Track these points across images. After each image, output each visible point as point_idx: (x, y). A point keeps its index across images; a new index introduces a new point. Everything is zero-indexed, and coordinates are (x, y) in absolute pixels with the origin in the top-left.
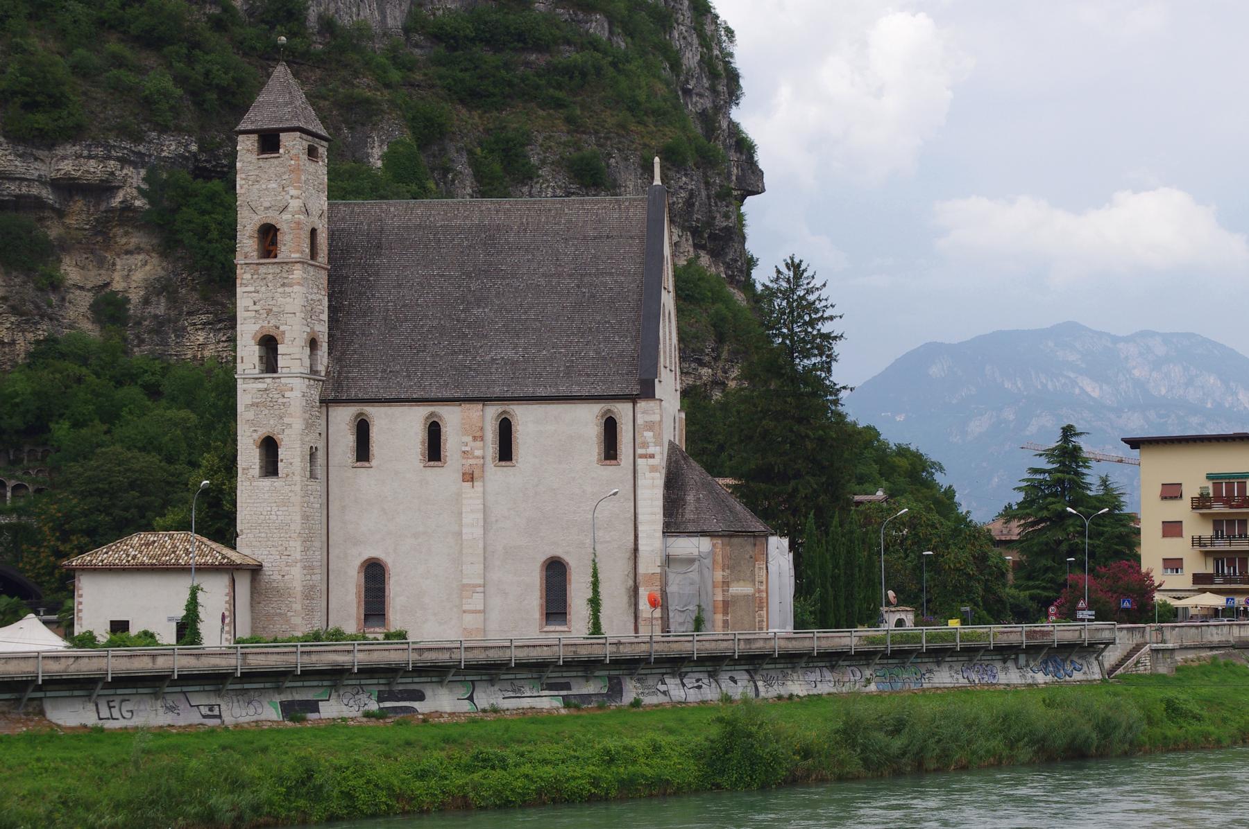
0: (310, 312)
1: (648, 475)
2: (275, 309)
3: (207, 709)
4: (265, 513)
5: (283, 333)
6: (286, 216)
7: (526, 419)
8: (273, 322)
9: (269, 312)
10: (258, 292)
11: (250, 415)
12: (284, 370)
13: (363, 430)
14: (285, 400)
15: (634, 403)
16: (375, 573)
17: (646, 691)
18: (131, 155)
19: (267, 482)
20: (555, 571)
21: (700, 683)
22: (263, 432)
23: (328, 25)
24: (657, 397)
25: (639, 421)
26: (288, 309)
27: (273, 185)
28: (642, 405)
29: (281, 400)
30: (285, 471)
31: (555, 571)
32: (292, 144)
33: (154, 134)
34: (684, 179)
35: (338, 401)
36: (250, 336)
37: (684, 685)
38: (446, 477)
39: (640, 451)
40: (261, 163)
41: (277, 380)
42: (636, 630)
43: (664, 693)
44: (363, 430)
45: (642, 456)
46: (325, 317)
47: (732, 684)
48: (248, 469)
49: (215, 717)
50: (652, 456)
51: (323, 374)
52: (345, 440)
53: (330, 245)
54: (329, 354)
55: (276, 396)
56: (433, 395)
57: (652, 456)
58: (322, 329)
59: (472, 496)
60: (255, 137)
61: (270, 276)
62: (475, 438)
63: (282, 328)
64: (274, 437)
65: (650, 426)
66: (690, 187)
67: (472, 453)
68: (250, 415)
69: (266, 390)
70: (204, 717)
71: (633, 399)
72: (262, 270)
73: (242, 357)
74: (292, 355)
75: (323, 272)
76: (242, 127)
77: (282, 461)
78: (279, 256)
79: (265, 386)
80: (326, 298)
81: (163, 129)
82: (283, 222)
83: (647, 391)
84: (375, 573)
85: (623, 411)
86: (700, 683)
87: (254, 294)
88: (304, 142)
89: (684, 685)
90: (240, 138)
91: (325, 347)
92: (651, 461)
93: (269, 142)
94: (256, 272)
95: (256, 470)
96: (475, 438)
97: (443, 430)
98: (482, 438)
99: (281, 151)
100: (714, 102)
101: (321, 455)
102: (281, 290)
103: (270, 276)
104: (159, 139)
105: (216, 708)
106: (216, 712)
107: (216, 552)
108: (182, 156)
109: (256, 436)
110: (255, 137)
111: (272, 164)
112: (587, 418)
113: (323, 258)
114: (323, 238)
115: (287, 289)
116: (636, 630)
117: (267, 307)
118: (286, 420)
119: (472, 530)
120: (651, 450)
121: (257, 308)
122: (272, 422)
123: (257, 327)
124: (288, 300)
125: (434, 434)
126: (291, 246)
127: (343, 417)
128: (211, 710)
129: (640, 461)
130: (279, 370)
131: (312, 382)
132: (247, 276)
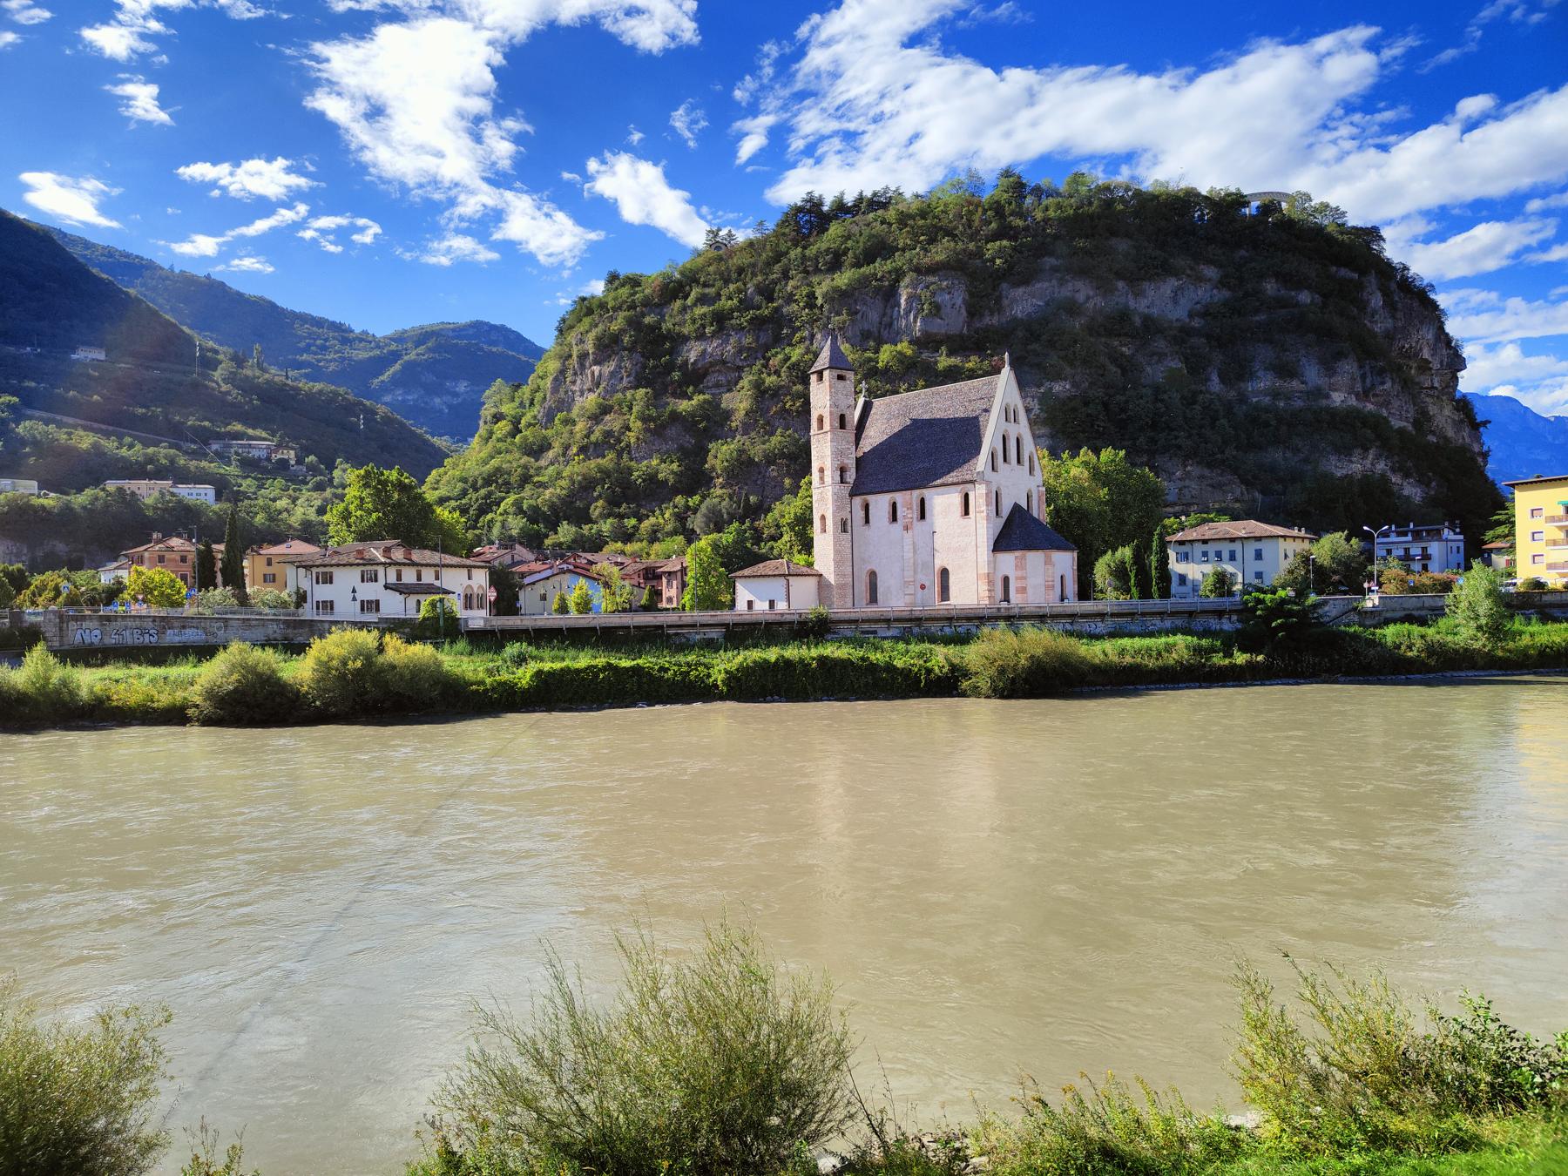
13: (867, 508)
38: (898, 526)
52: (859, 514)
59: (908, 537)
119: (909, 555)
125: (894, 506)
127: (858, 501)
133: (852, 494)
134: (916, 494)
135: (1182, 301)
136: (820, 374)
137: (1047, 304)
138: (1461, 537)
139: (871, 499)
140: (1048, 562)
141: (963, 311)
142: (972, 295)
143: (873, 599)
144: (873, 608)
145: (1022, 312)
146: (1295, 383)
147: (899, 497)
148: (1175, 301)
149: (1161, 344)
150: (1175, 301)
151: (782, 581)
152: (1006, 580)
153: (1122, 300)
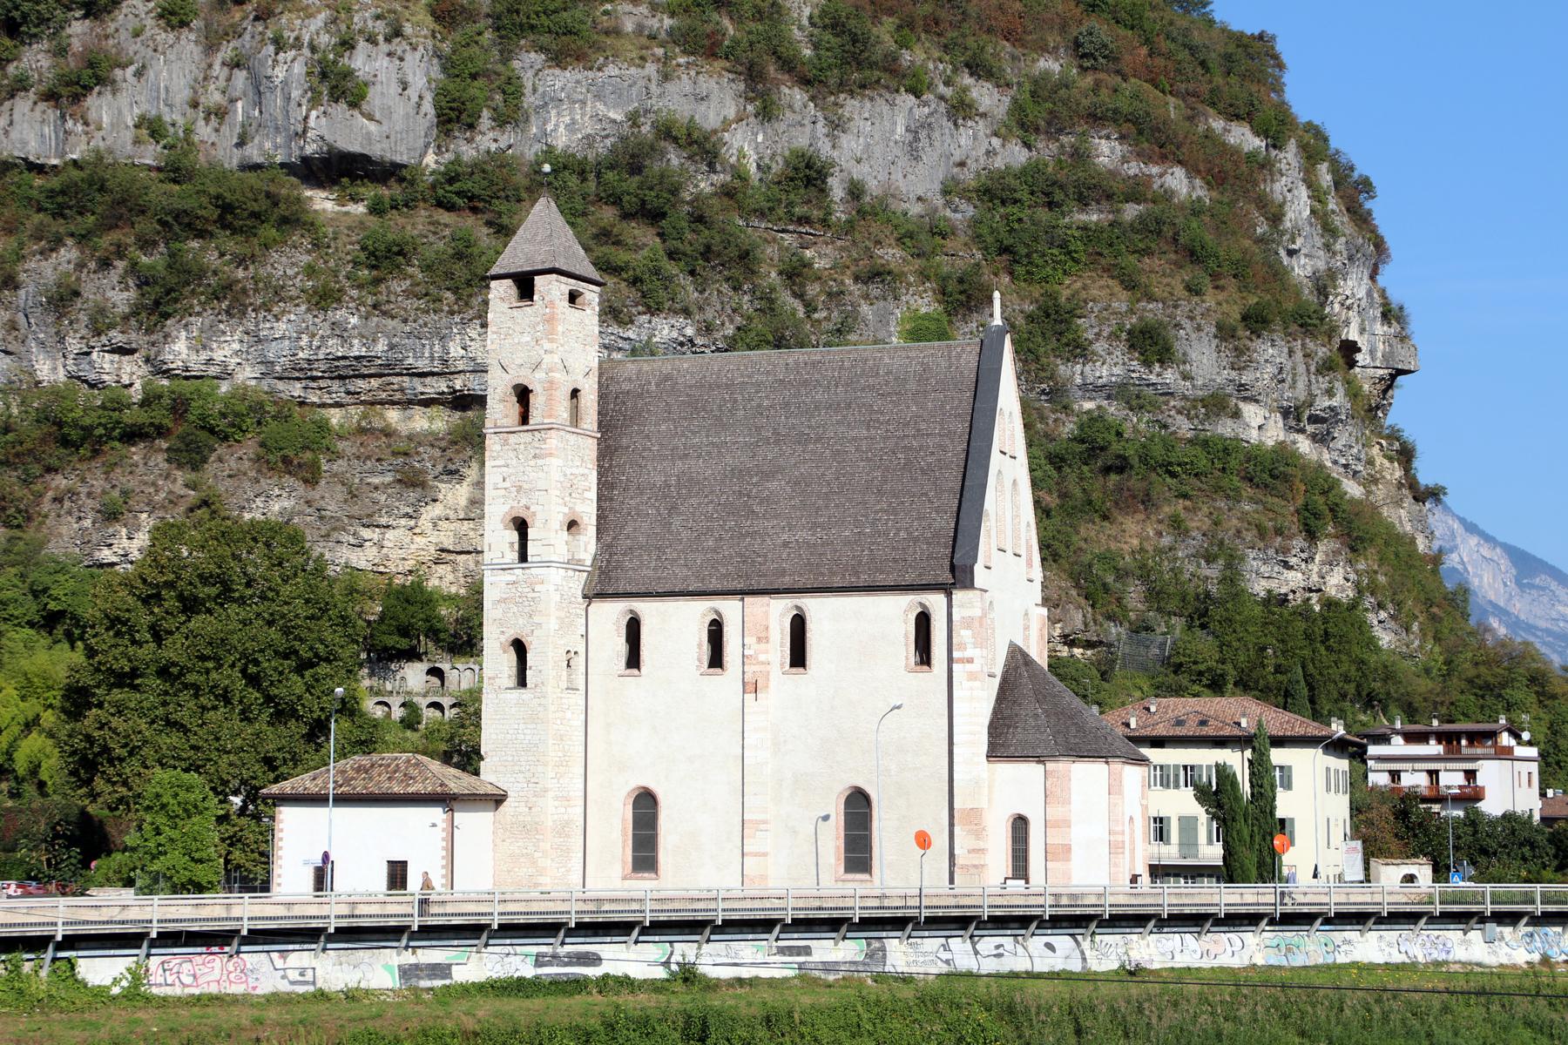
0: (571, 488)
1: (967, 684)
2: (525, 486)
3: (297, 972)
5: (534, 514)
6: (540, 375)
7: (821, 611)
8: (523, 502)
9: (519, 489)
10: (507, 466)
12: (535, 559)
13: (633, 629)
15: (949, 595)
16: (646, 805)
17: (921, 959)
18: (619, 341)
20: (858, 805)
21: (1001, 950)
22: (511, 634)
23: (855, 191)
24: (977, 584)
25: (955, 617)
26: (541, 486)
27: (526, 338)
28: (959, 596)
29: (530, 595)
30: (534, 681)
31: (858, 805)
32: (551, 289)
33: (646, 317)
34: (1270, 351)
35: (602, 595)
36: (499, 518)
37: (976, 953)
39: (956, 654)
42: (952, 881)
43: (947, 962)
44: (633, 629)
45: (961, 661)
46: (593, 495)
47: (1049, 953)
49: (306, 983)
50: (970, 661)
51: (589, 563)
53: (601, 413)
54: (598, 539)
56: (711, 587)
57: (970, 661)
58: (588, 513)
61: (522, 447)
62: (759, 640)
63: (533, 509)
65: (968, 623)
66: (1278, 360)
67: (756, 658)
69: (514, 583)
70: (293, 983)
71: (947, 589)
72: (513, 439)
74: (547, 539)
75: (590, 441)
76: (494, 270)
78: (531, 422)
79: (514, 578)
80: (595, 473)
81: (653, 310)
82: (535, 382)
83: (958, 576)
84: (646, 805)
85: (935, 602)
86: (1001, 950)
87: (505, 469)
88: (563, 286)
89: (976, 953)
90: (493, 284)
91: (592, 531)
92: (968, 666)
93: (525, 286)
94: (506, 443)
96: (759, 640)
97: (725, 629)
98: (767, 640)
99: (535, 297)
100: (1328, 263)
101: (579, 662)
102: (532, 463)
103: (522, 447)
104: (650, 322)
105: (310, 973)
106: (309, 976)
107: (456, 780)
108: (675, 340)
109: (503, 639)
110: (509, 282)
111: (529, 314)
112: (897, 611)
113: (590, 420)
114: (590, 400)
115: (540, 462)
116: (952, 881)
118: (536, 619)
120: (968, 653)
121: (507, 484)
122: (521, 621)
123: (506, 508)
124: (541, 474)
126: (549, 406)
127: (612, 615)
128: (302, 975)
129: (955, 667)
130: (529, 559)
131: (570, 573)
132: (498, 447)
133: (598, 591)
134: (776, 612)
135: (929, 156)
136: (525, 286)
137: (633, 118)
138: (1533, 752)
139: (649, 610)
140: (1114, 788)
141: (428, 107)
142: (450, 66)
143: (645, 855)
144: (643, 885)
145: (572, 127)
146: (1170, 376)
147: (730, 608)
148: (914, 154)
149: (891, 255)
150: (914, 154)
151: (436, 813)
152: (1020, 825)
153: (802, 141)
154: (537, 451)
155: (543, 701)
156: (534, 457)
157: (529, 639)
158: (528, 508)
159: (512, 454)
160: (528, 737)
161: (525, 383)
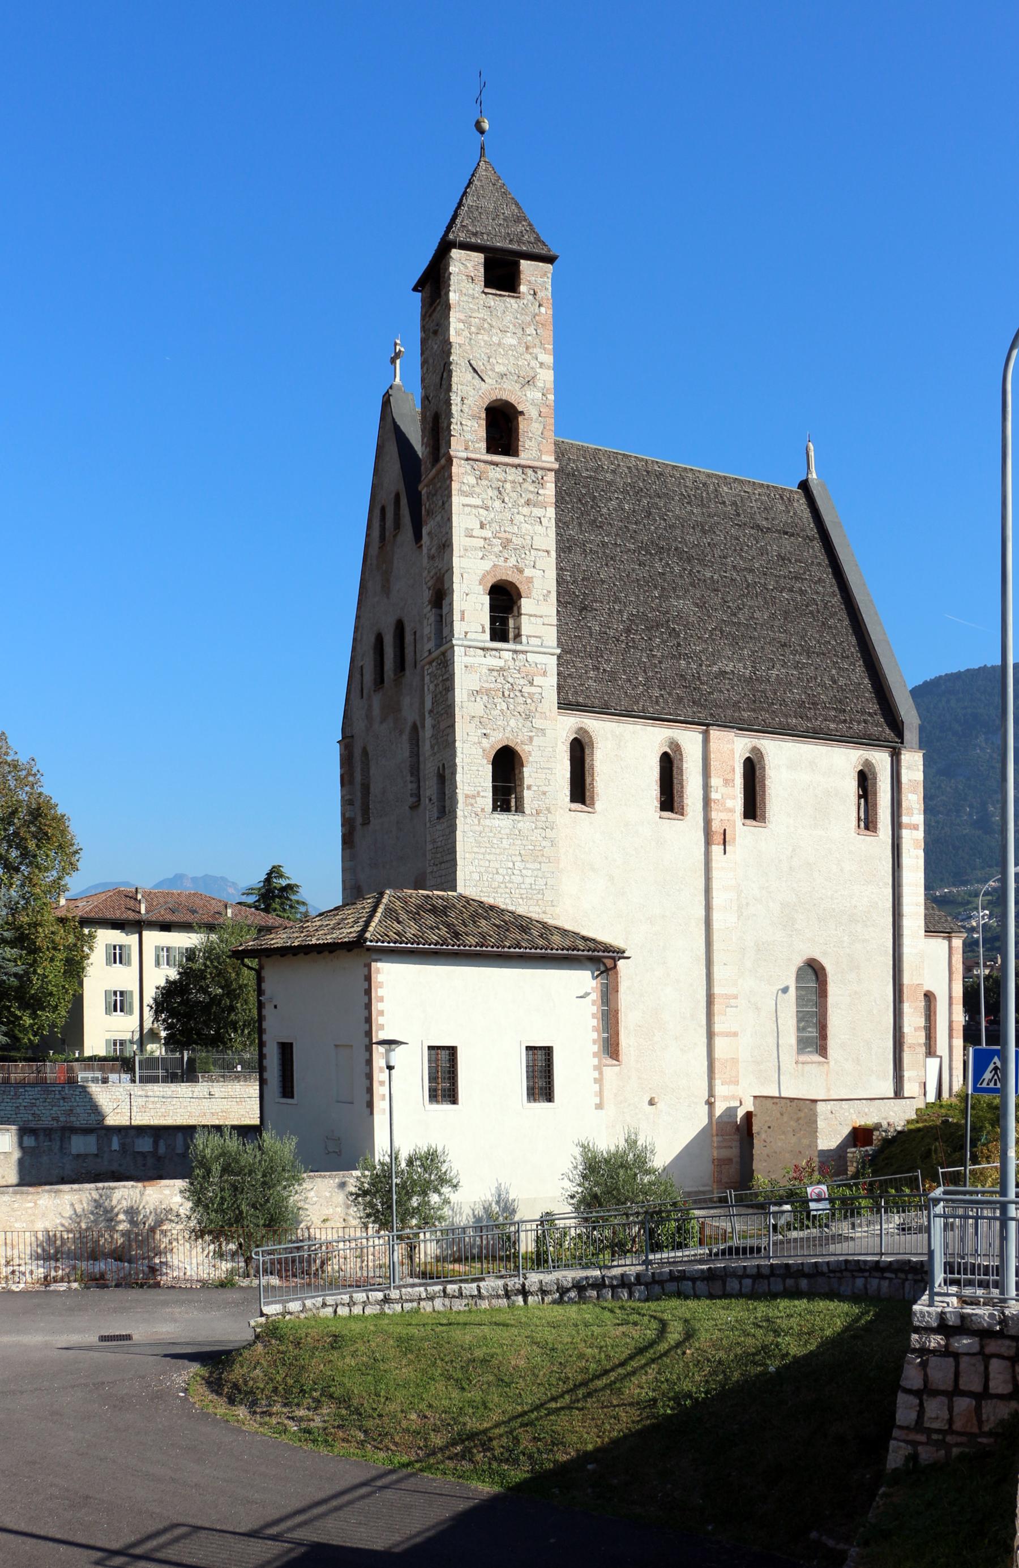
4: (501, 871)
5: (530, 580)
8: (512, 561)
9: (506, 544)
10: (487, 509)
11: (477, 708)
14: (533, 690)
19: (504, 821)
30: (536, 804)
40: (491, 301)
41: (521, 656)
48: (474, 797)
55: (522, 682)
60: (479, 258)
63: (528, 572)
64: (518, 749)
68: (477, 708)
69: (502, 669)
73: (463, 613)
77: (529, 788)
78: (522, 454)
79: (501, 663)
87: (482, 511)
95: (487, 799)
99: (523, 288)
102: (525, 510)
110: (479, 258)
117: (502, 535)
123: (487, 565)
130: (524, 639)
154: (531, 496)
155: (549, 833)
156: (528, 503)
157: (526, 748)
158: (521, 571)
159: (491, 493)
160: (528, 880)
161: (512, 400)
